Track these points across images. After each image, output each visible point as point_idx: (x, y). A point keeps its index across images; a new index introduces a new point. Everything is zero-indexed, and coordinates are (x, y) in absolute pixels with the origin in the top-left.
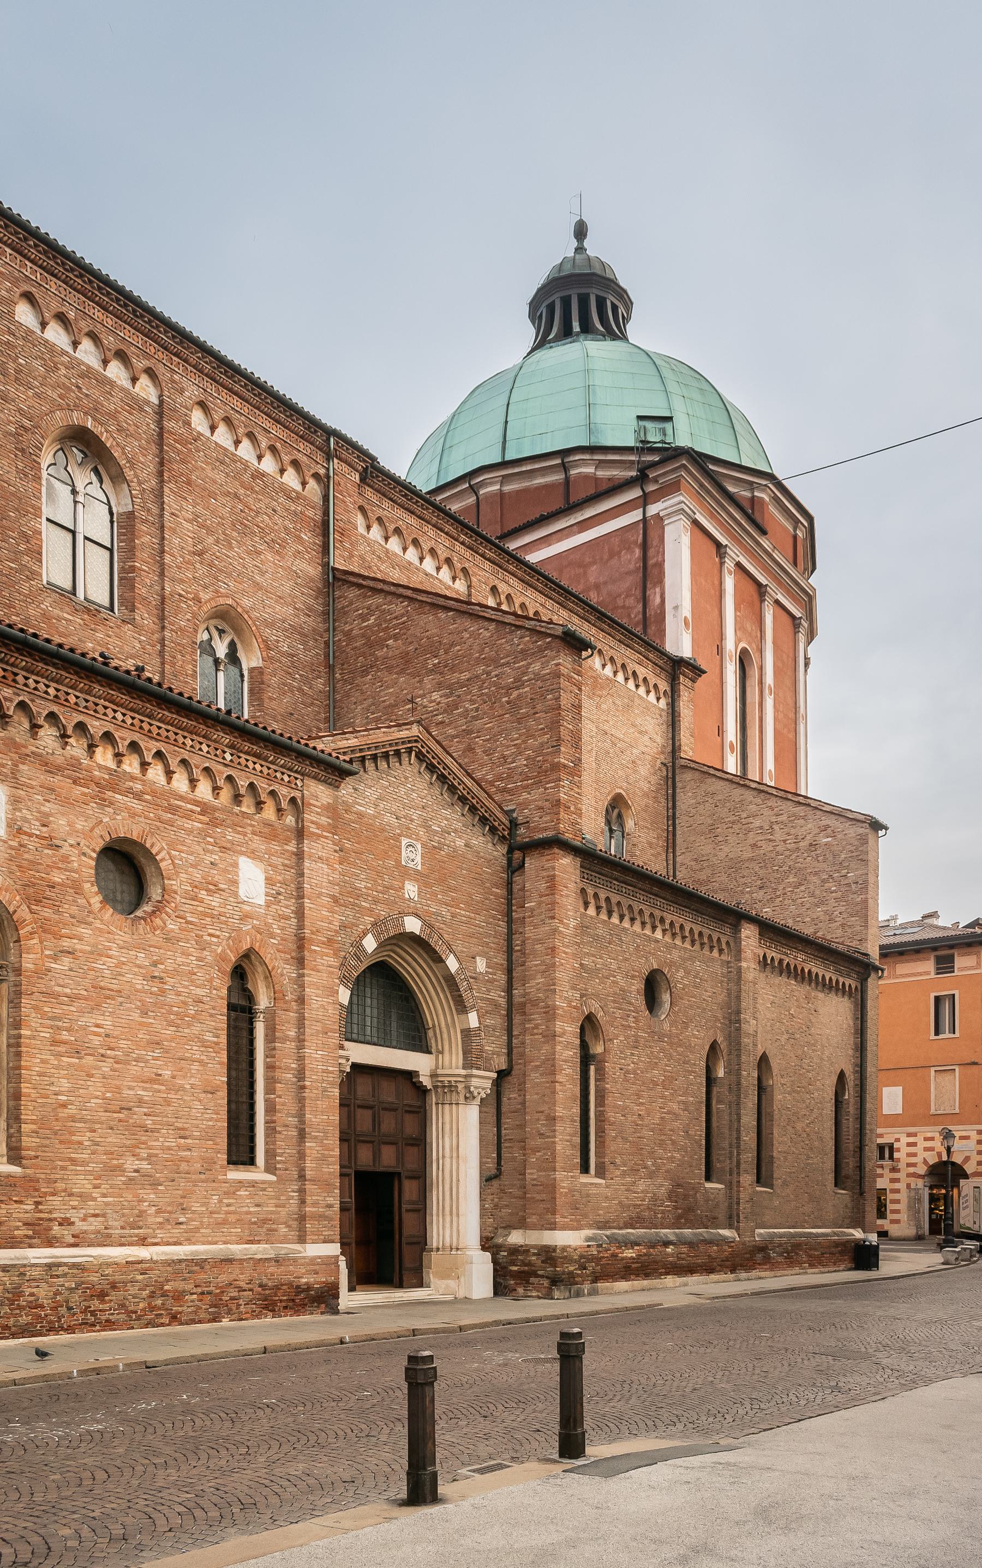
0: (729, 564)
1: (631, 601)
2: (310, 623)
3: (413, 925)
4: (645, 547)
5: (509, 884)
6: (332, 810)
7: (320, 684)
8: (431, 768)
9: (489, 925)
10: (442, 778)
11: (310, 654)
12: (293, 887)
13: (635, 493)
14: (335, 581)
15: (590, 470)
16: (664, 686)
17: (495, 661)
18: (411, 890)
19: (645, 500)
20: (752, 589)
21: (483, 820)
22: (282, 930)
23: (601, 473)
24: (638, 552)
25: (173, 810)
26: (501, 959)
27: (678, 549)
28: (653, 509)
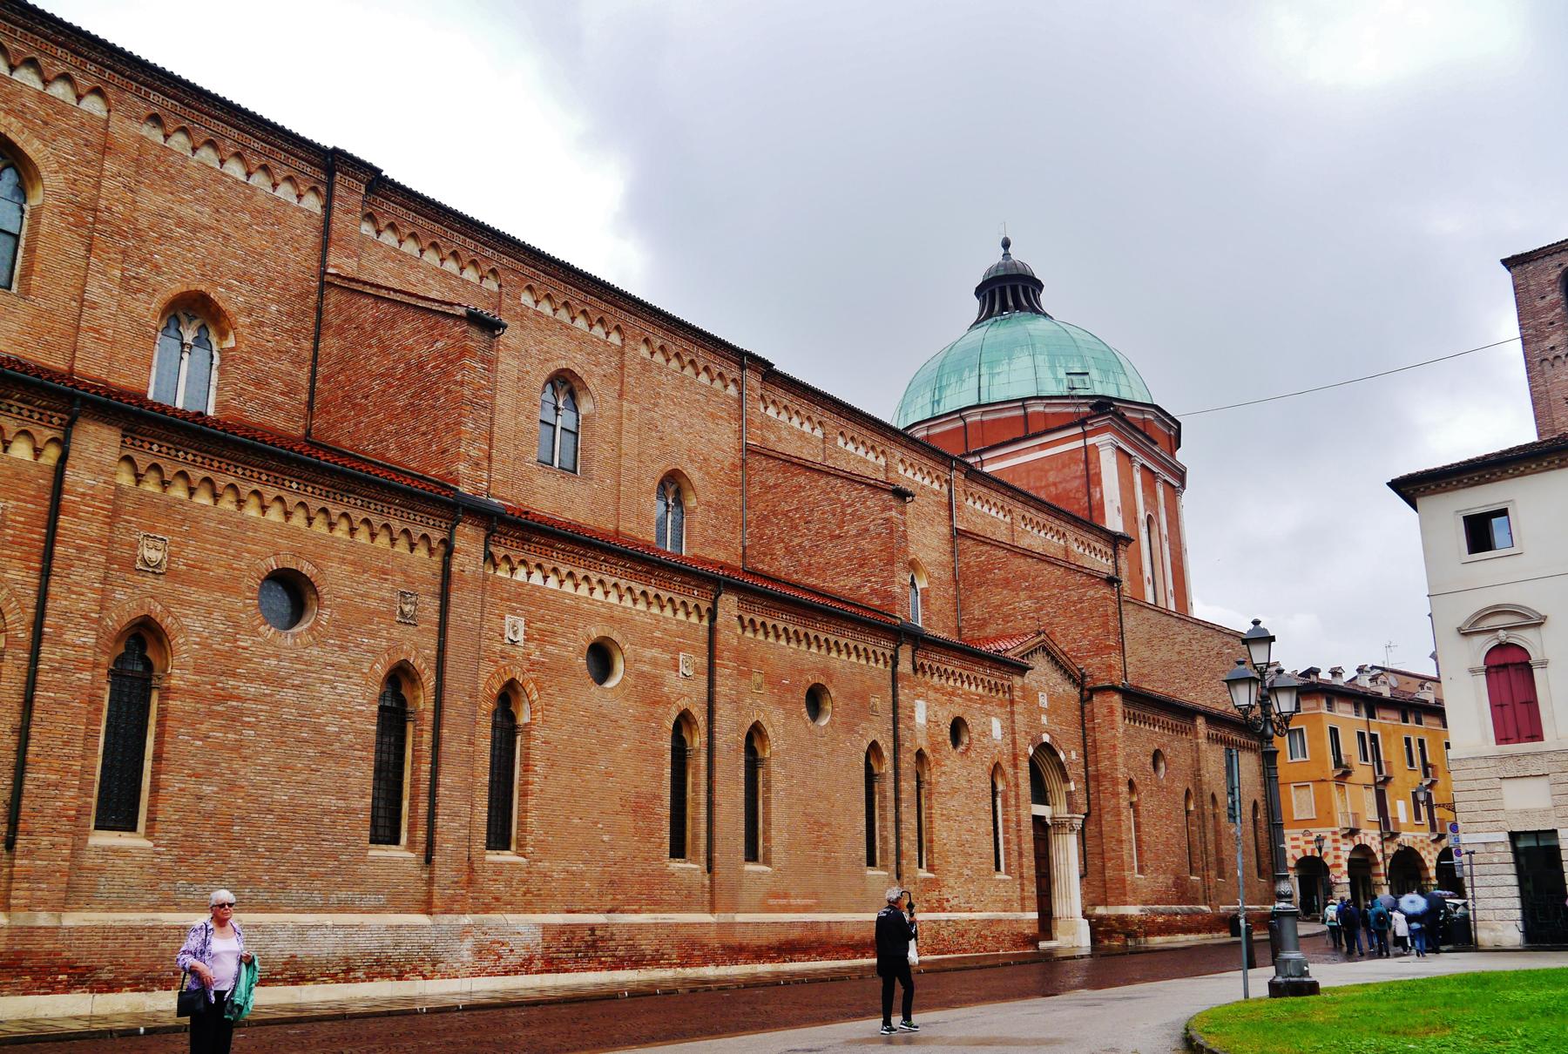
0: (1137, 466)
1: (1079, 495)
2: (947, 558)
3: (1046, 738)
4: (1087, 462)
5: (1082, 709)
6: (1023, 688)
7: (951, 591)
8: (1048, 654)
9: (1075, 733)
10: (1053, 658)
11: (946, 576)
12: (1010, 730)
13: (1079, 430)
14: (958, 535)
15: (1041, 409)
16: (1110, 552)
17: (1065, 588)
18: (1044, 719)
19: (1085, 435)
20: (1149, 476)
21: (1070, 676)
22: (1007, 750)
23: (1048, 410)
24: (1082, 466)
25: (971, 700)
26: (1081, 751)
27: (1108, 465)
28: (1090, 441)
